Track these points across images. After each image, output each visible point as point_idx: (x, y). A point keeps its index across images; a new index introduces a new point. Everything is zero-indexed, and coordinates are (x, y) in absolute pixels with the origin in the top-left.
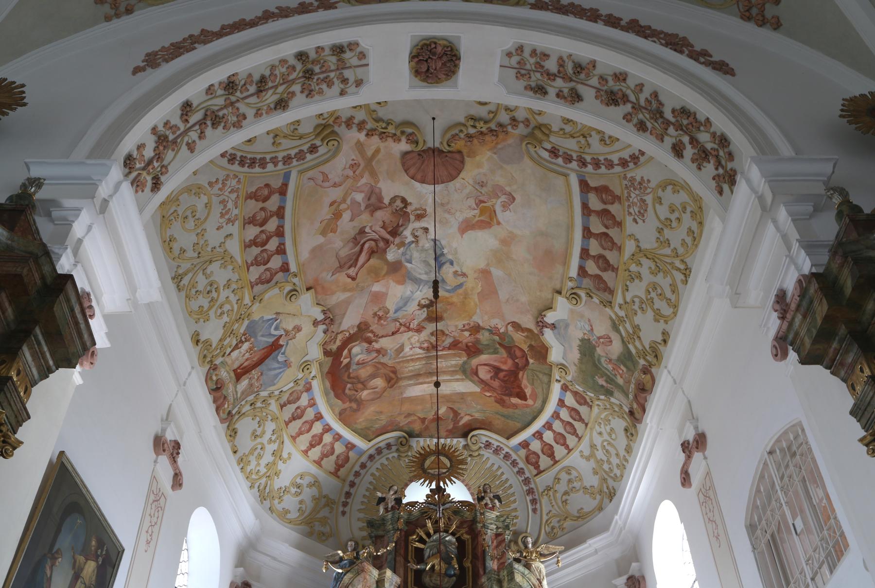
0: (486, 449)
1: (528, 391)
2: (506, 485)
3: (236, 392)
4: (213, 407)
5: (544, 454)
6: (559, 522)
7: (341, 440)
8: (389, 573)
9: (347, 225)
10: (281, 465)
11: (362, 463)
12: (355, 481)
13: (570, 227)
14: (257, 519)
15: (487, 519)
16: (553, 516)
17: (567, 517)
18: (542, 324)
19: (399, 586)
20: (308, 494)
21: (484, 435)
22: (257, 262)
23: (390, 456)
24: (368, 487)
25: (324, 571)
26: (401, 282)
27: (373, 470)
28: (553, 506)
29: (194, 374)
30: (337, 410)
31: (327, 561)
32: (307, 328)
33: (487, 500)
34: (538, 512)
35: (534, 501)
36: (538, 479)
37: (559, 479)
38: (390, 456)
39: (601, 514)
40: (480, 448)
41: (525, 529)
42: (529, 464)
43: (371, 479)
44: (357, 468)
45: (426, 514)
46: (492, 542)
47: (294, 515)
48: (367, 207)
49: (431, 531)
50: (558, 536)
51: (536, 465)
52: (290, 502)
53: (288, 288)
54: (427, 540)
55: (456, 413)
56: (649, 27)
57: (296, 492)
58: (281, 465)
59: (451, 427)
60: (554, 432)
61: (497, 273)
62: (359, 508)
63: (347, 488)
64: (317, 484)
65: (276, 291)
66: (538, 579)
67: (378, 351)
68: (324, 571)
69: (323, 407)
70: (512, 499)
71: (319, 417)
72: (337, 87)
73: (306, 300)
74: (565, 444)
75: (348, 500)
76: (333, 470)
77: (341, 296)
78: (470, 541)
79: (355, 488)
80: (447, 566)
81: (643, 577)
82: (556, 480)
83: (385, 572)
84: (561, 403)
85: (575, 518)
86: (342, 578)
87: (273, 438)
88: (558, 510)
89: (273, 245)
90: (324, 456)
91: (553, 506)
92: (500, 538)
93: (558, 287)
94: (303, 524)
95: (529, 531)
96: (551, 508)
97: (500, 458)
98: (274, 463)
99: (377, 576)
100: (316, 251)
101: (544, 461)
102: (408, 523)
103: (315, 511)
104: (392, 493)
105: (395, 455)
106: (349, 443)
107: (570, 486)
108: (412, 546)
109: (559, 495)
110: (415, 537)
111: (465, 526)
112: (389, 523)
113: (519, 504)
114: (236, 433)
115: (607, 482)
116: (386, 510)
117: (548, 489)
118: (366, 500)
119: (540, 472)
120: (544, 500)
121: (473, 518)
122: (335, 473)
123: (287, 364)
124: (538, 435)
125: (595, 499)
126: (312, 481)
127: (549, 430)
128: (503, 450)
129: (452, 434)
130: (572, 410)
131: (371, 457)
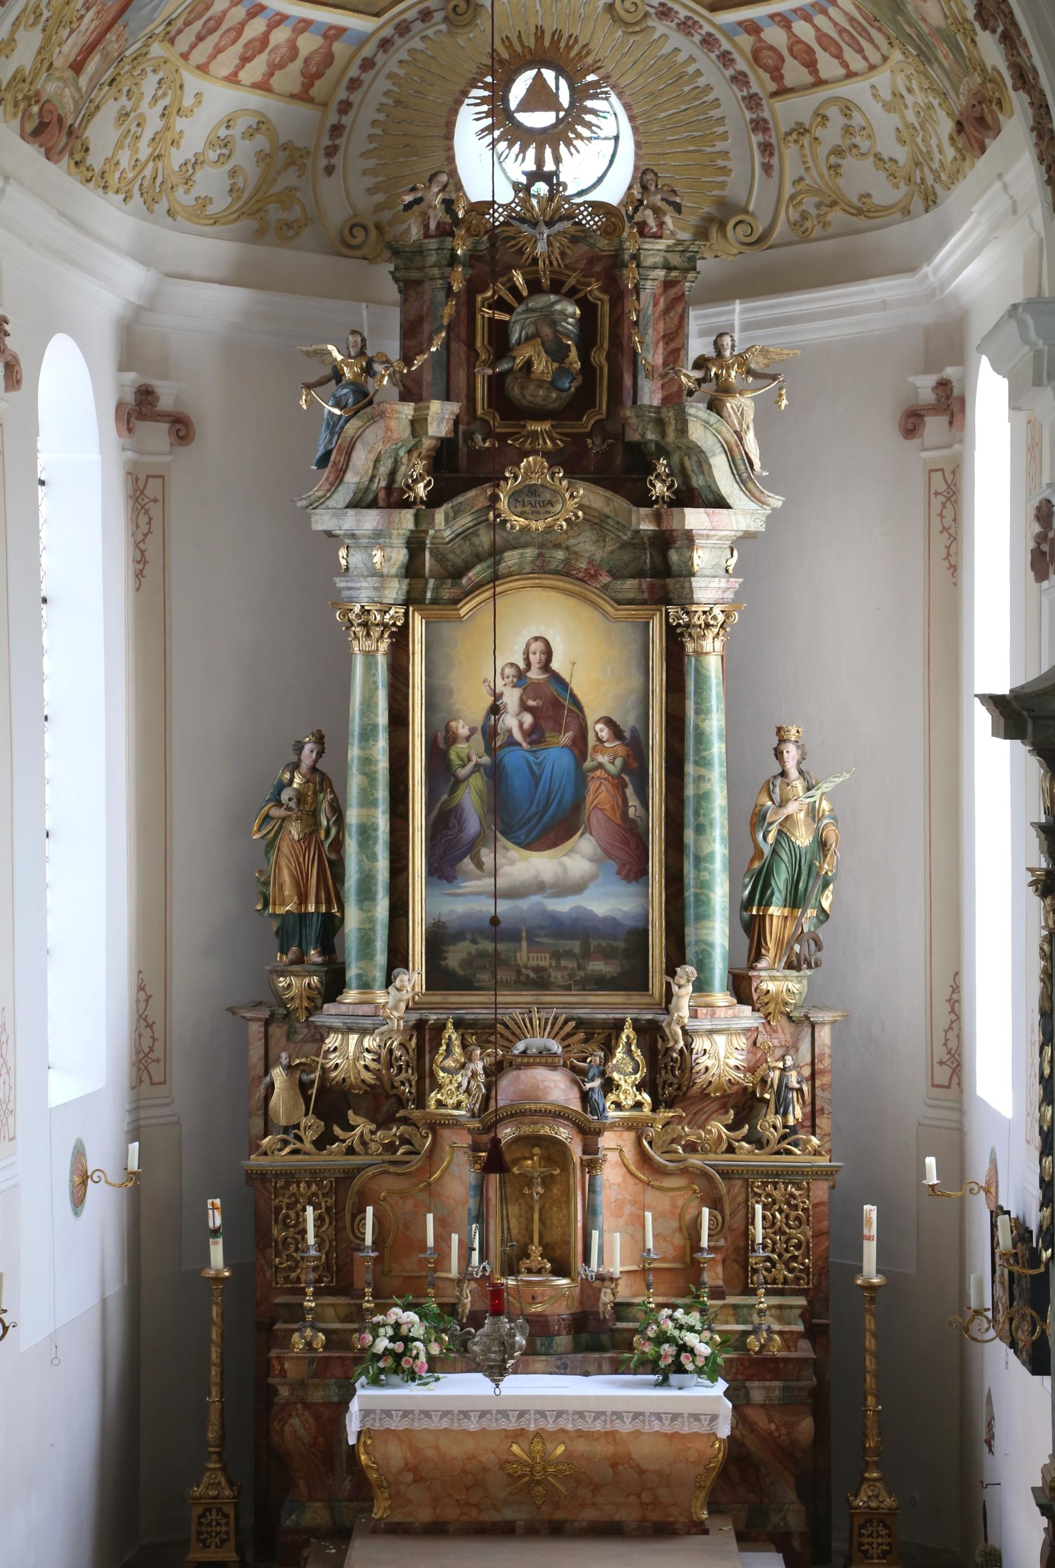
0: (661, 20)
2: (705, 99)
3: (79, 89)
5: (795, 58)
6: (818, 206)
7: (312, 28)
8: (435, 406)
10: (180, 123)
11: (365, 59)
12: (352, 98)
14: (148, 271)
15: (646, 257)
16: (807, 191)
17: (834, 204)
19: (458, 416)
20: (245, 153)
23: (430, 33)
24: (381, 104)
25: (304, 407)
27: (392, 66)
28: (807, 169)
31: (309, 387)
34: (775, 173)
35: (766, 148)
37: (825, 118)
38: (430, 33)
39: (904, 227)
40: (646, 15)
41: (744, 199)
42: (761, 67)
44: (354, 71)
45: (513, 243)
46: (655, 304)
47: (221, 204)
49: (525, 293)
50: (813, 236)
51: (776, 74)
54: (515, 304)
57: (219, 155)
60: (817, 29)
62: (364, 150)
63: (333, 118)
64: (263, 127)
66: (736, 432)
68: (304, 407)
70: (720, 130)
75: (337, 142)
76: (296, 88)
78: (607, 307)
79: (352, 113)
80: (556, 365)
81: (962, 400)
82: (819, 119)
83: (428, 408)
85: (854, 211)
86: (342, 428)
87: (160, 93)
88: (818, 180)
90: (273, 68)
91: (807, 169)
92: (673, 292)
94: (242, 217)
95: (751, 208)
96: (803, 173)
97: (694, 43)
98: (167, 128)
99: (412, 412)
101: (794, 72)
102: (473, 258)
103: (265, 181)
104: (435, 189)
105: (443, 27)
106: (331, 27)
107: (848, 142)
108: (483, 316)
109: (823, 150)
110: (489, 294)
111: (598, 269)
112: (433, 258)
114: (87, 150)
115: (922, 171)
116: (427, 236)
117: (801, 130)
118: (378, 131)
119: (782, 91)
120: (790, 153)
121: (616, 250)
122: (304, 96)
125: (898, 187)
126: (253, 121)
127: (806, 21)
128: (701, 27)
131: (385, 44)
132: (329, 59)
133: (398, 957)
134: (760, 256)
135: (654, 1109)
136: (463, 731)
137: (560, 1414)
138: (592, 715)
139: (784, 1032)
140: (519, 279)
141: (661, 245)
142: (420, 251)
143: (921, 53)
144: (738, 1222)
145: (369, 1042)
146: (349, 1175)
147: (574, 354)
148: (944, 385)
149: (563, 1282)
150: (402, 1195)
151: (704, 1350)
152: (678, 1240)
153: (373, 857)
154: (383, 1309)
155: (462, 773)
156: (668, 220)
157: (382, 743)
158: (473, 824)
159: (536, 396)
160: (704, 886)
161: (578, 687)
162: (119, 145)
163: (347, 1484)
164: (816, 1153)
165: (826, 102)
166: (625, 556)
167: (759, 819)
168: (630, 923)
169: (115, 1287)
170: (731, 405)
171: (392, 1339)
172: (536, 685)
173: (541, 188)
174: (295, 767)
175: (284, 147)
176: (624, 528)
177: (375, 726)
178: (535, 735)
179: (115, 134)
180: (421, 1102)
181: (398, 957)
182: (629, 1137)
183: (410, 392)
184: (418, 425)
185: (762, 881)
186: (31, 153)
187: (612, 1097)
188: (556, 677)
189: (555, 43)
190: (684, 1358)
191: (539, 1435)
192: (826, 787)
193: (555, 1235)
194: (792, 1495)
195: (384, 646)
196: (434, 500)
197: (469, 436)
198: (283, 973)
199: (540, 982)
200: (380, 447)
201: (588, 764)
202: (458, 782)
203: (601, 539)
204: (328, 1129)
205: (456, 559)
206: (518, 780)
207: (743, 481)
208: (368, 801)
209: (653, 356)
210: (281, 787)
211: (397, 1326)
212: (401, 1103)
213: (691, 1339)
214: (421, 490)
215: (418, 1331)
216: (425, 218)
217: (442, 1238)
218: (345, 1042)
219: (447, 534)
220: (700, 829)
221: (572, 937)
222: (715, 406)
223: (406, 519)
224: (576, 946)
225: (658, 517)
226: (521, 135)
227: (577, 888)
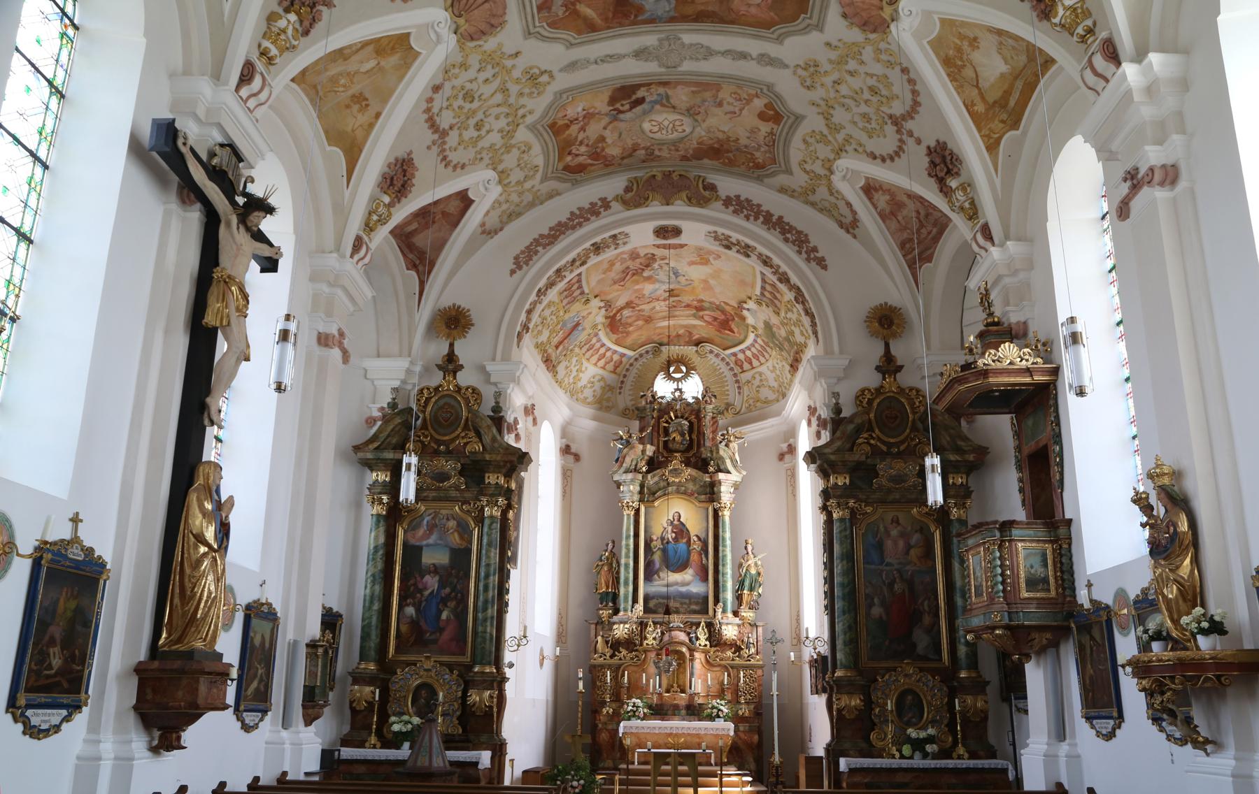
1: (736, 330)
4: (545, 368)
8: (649, 446)
9: (618, 267)
10: (581, 375)
13: (755, 276)
18: (741, 308)
20: (598, 386)
21: (708, 347)
22: (566, 297)
26: (654, 283)
27: (638, 366)
29: (539, 369)
30: (614, 340)
32: (595, 311)
33: (707, 398)
35: (739, 388)
36: (742, 375)
43: (636, 371)
44: (627, 366)
48: (630, 259)
52: (588, 393)
53: (583, 300)
55: (690, 333)
56: (788, 224)
58: (581, 375)
59: (687, 339)
61: (712, 282)
65: (578, 303)
67: (639, 311)
69: (605, 340)
71: (603, 345)
72: (613, 247)
73: (596, 303)
74: (758, 360)
76: (612, 369)
77: (615, 294)
81: (795, 448)
84: (755, 341)
89: (575, 287)
90: (607, 363)
93: (750, 295)
98: (578, 375)
100: (599, 282)
101: (746, 366)
102: (659, 410)
103: (603, 394)
109: (754, 387)
113: (731, 388)
117: (748, 382)
119: (743, 371)
120: (746, 388)
122: (614, 372)
123: (583, 329)
124: (743, 351)
129: (688, 343)
130: (761, 346)
131: (636, 359)
132: (621, 362)
133: (635, 601)
134: (738, 417)
135: (711, 646)
136: (655, 538)
137: (683, 728)
138: (692, 534)
139: (747, 629)
140: (672, 414)
141: (711, 407)
142: (645, 409)
143: (780, 348)
144: (736, 682)
145: (627, 626)
146: (620, 666)
147: (687, 435)
148: (790, 445)
149: (683, 695)
150: (636, 672)
151: (726, 710)
152: (718, 686)
153: (629, 573)
154: (630, 698)
155: (654, 550)
156: (713, 400)
157: (632, 541)
158: (657, 565)
159: (677, 446)
160: (725, 582)
161: (688, 526)
162: (565, 376)
163: (618, 755)
164: (758, 661)
165: (756, 373)
166: (701, 489)
167: (741, 565)
168: (703, 594)
169: (550, 699)
170: (731, 445)
171: (633, 707)
172: (676, 525)
173: (677, 394)
174: (606, 550)
175: (609, 386)
176: (701, 481)
177: (630, 536)
178: (676, 540)
179: (565, 372)
180: (641, 645)
181: (635, 601)
182: (703, 655)
183: (641, 440)
184: (643, 452)
185: (742, 584)
186: (543, 366)
187: (698, 642)
188: (682, 523)
189: (682, 357)
190: (720, 713)
191: (676, 735)
192: (759, 557)
193: (681, 683)
194: (752, 760)
195: (633, 513)
196: (648, 472)
197: (658, 457)
198: (602, 609)
199: (677, 612)
200: (633, 456)
201: (691, 548)
202: (653, 553)
203: (695, 485)
204: (614, 653)
205: (654, 490)
206: (671, 553)
207: (735, 467)
208: (627, 556)
209: (708, 432)
210: (602, 556)
211: (634, 703)
212: (635, 645)
213: (722, 708)
214: (644, 469)
215: (641, 704)
216: (646, 399)
217: (648, 681)
218: (619, 627)
219: (651, 483)
220: (723, 565)
221: (686, 598)
222: (727, 445)
223: (640, 477)
224: (687, 601)
225: (711, 477)
226: (675, 380)
227: (688, 584)
